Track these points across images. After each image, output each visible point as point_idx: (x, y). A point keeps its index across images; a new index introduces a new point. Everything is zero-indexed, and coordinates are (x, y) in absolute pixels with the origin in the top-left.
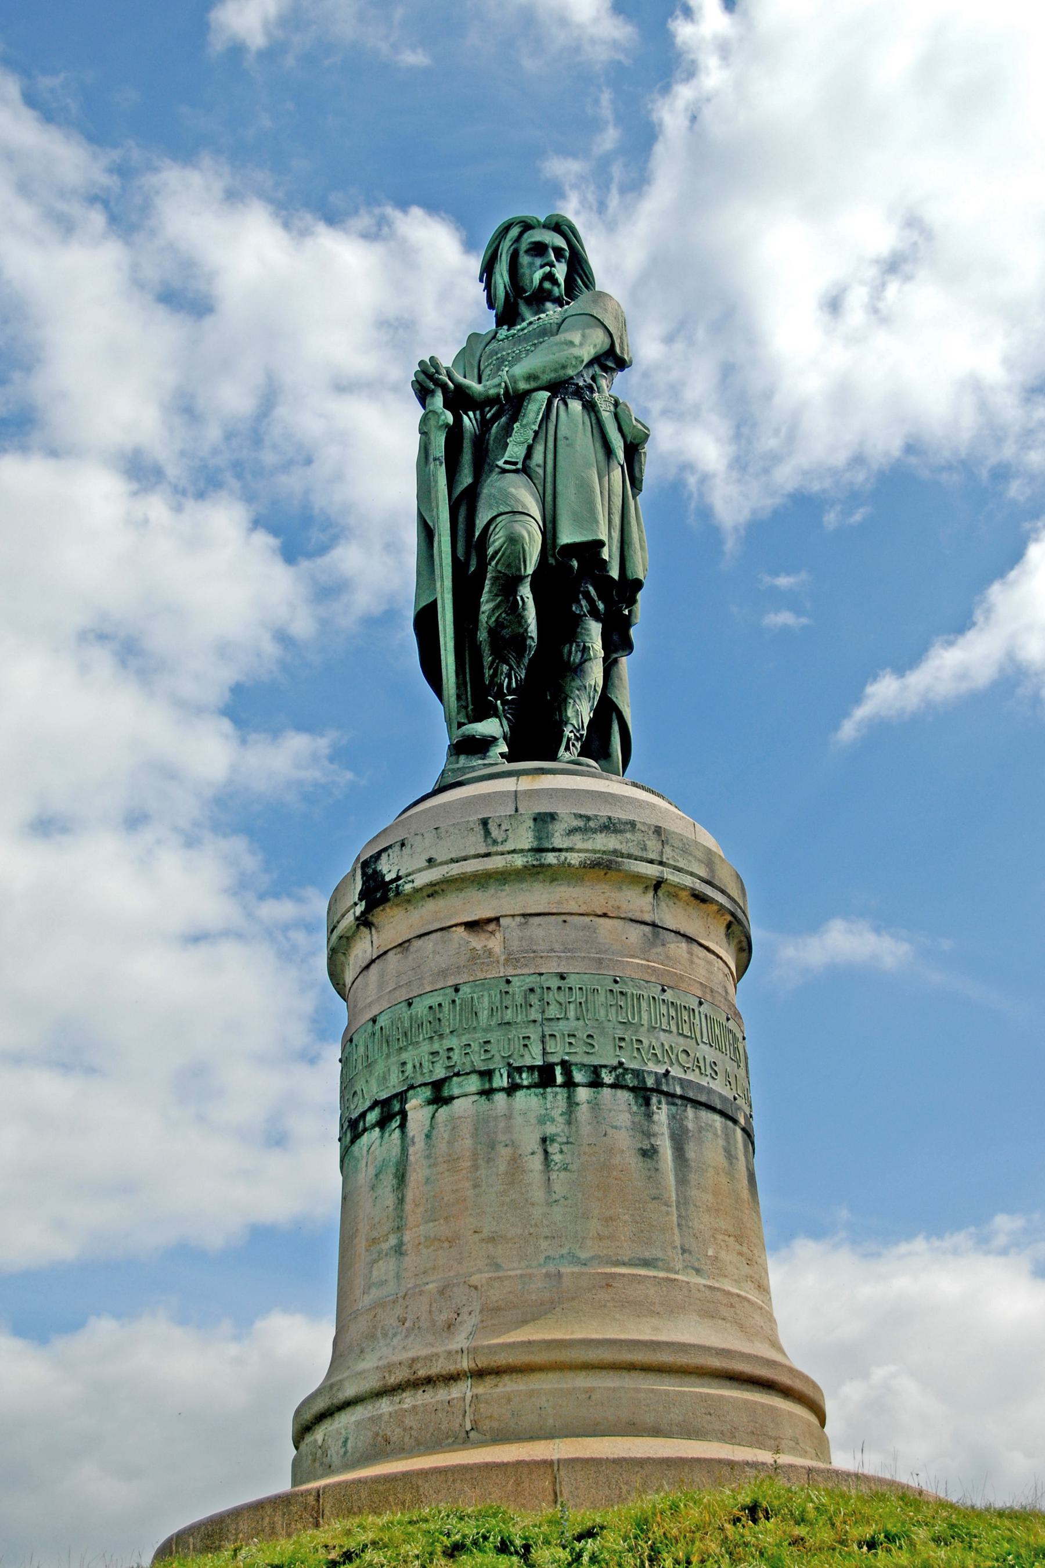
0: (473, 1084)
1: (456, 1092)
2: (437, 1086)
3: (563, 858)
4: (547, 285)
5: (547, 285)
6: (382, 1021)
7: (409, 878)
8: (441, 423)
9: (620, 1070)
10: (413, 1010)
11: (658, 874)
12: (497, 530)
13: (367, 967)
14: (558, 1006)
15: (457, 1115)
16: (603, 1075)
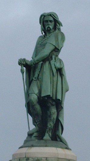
5: (49, 29)
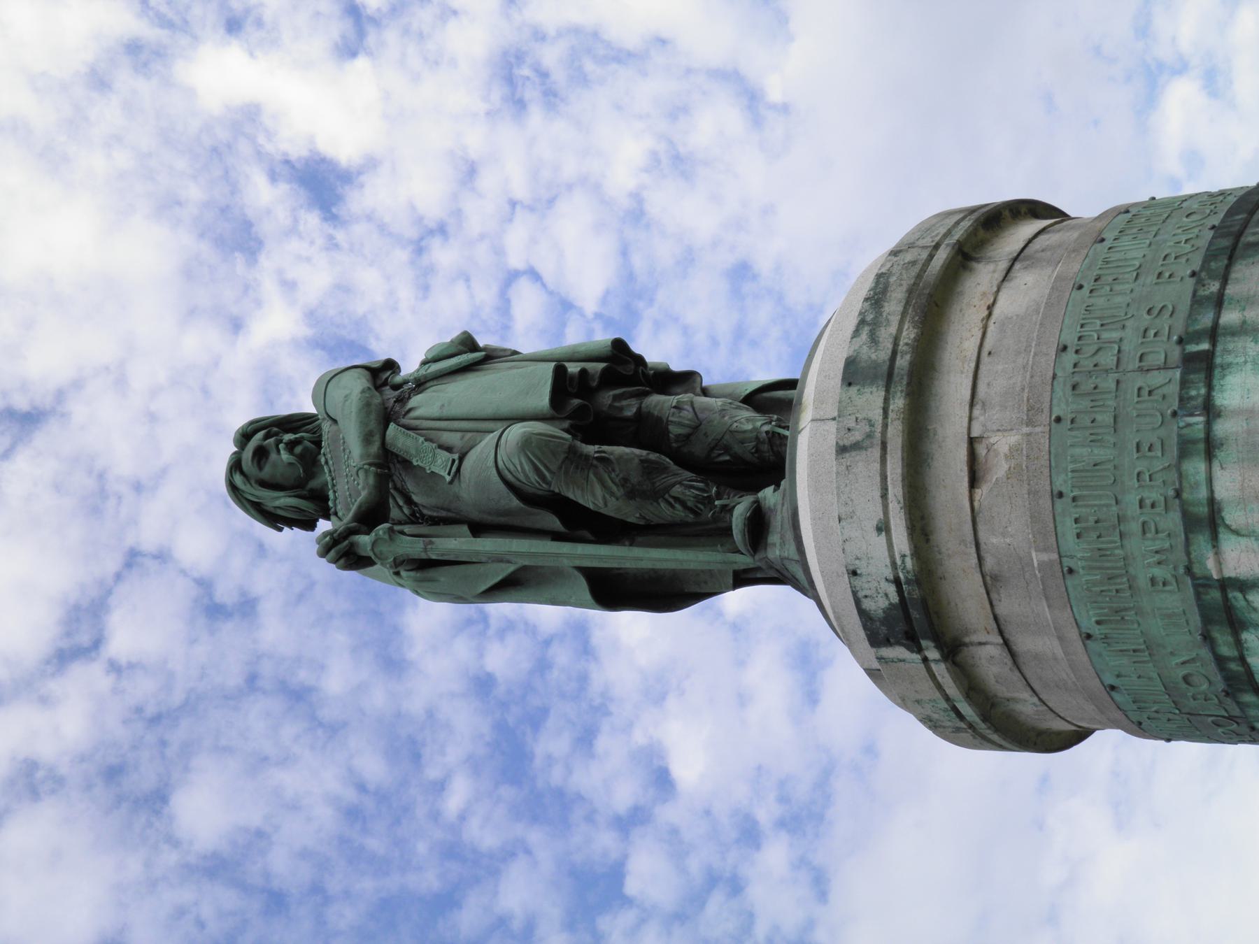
0: (1196, 467)
1: (1203, 493)
2: (1191, 523)
3: (905, 348)
4: (298, 449)
6: (1089, 624)
7: (899, 562)
8: (386, 537)
9: (1203, 274)
10: (1077, 565)
11: (949, 249)
12: (512, 468)
13: (1013, 655)
14: (1100, 353)
15: (1238, 493)
16: (1207, 293)
